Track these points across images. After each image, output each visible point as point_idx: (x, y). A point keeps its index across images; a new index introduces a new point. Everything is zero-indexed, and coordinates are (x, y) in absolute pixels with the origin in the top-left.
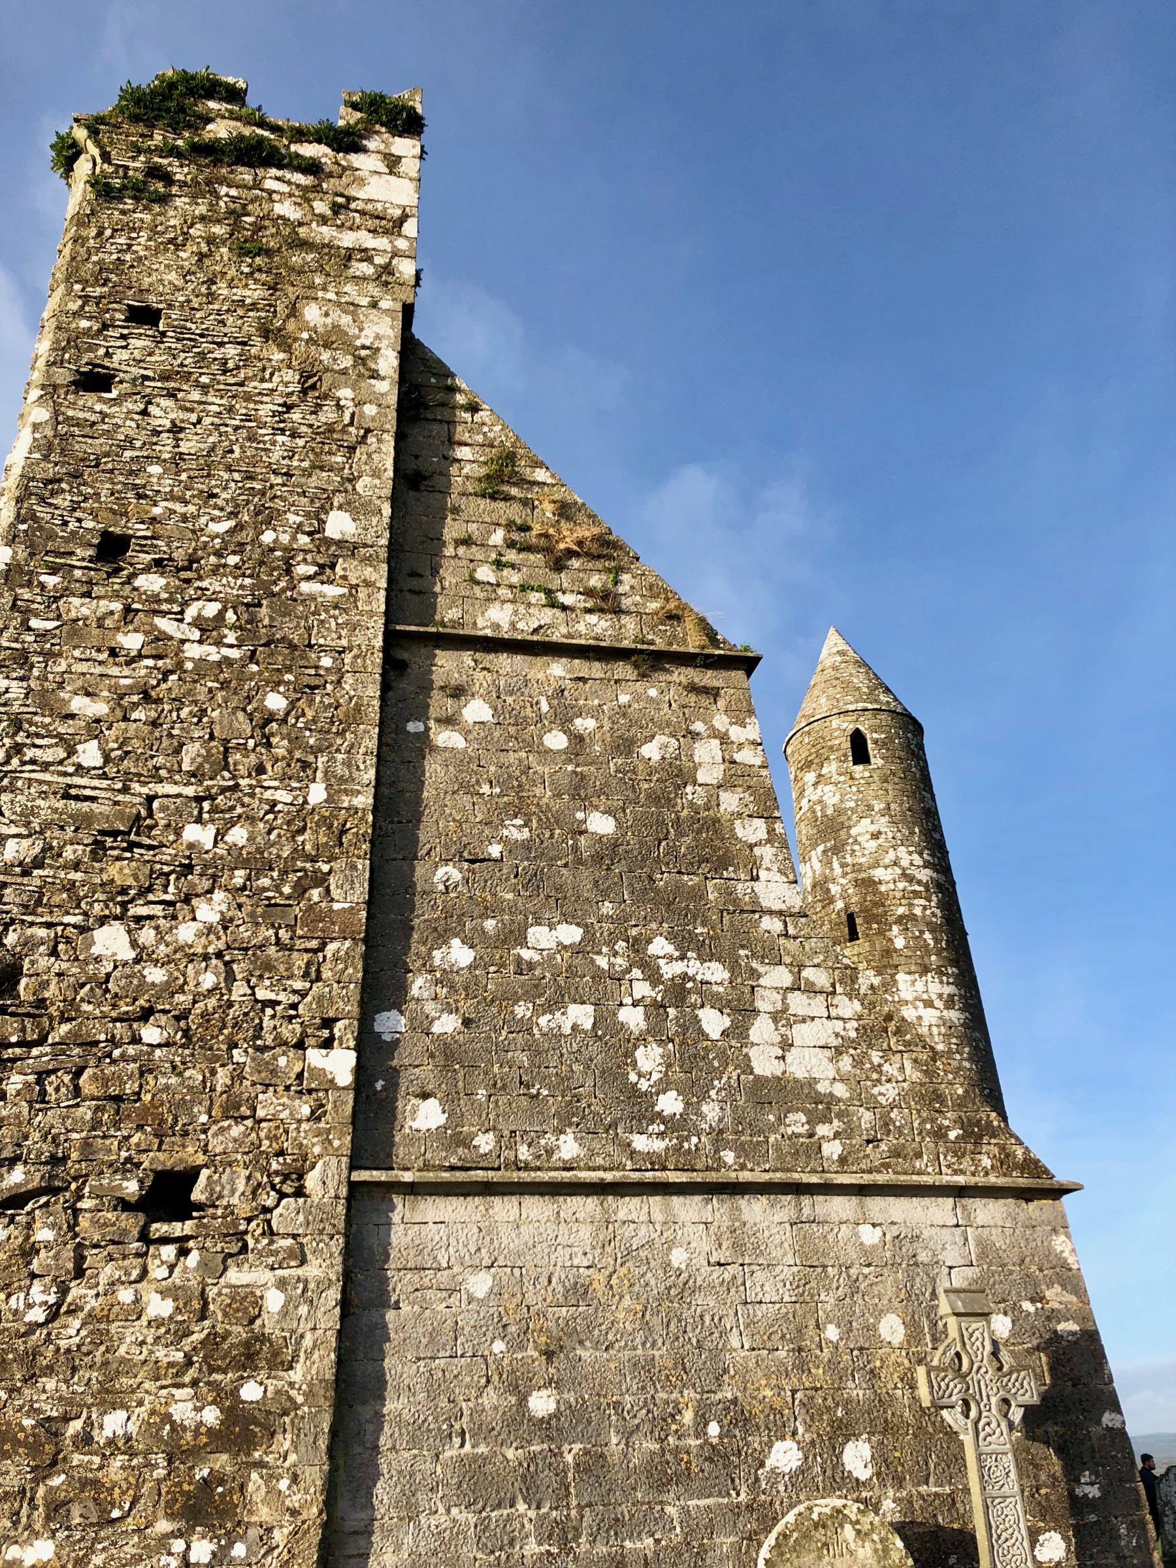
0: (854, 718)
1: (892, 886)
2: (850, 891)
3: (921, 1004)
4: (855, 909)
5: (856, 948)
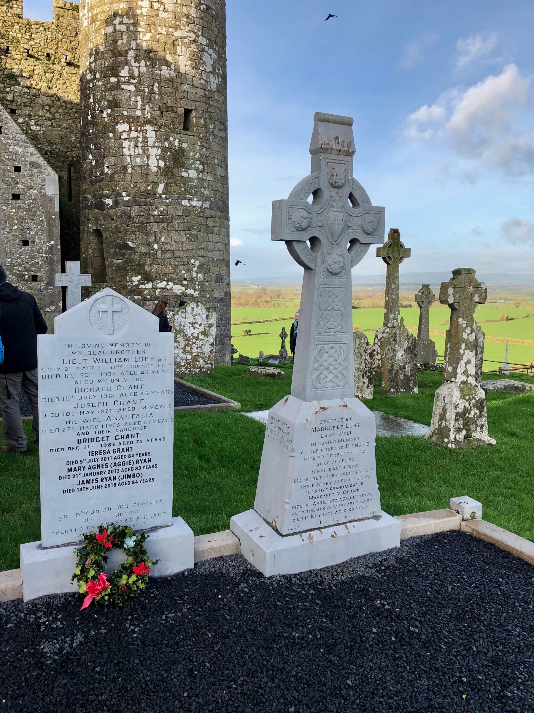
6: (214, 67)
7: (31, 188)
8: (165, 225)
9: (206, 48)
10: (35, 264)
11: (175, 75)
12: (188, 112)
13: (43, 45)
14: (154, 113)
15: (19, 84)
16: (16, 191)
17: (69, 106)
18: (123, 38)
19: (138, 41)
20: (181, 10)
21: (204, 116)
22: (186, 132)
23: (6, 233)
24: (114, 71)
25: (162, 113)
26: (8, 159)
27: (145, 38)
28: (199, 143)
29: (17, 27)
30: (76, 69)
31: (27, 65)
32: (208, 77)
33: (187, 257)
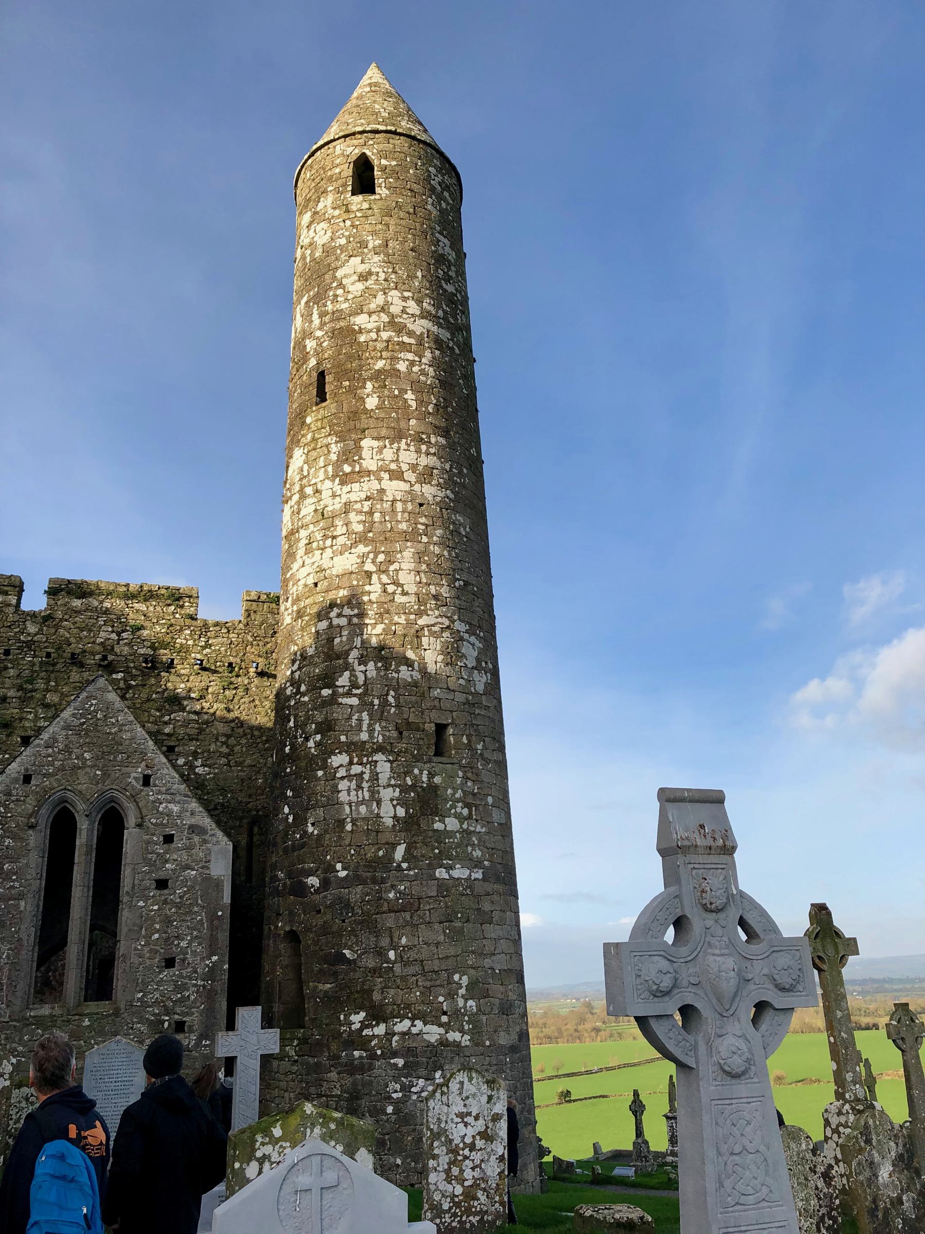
0: (362, 141)
1: (373, 335)
2: (325, 344)
3: (386, 476)
4: (327, 365)
5: (321, 411)
6: (478, 660)
7: (188, 867)
8: (407, 916)
9: (466, 636)
11: (419, 677)
12: (441, 729)
13: (223, 653)
14: (387, 734)
15: (183, 709)
16: (162, 875)
17: (256, 733)
18: (343, 634)
19: (365, 637)
20: (427, 590)
21: (467, 732)
22: (440, 759)
23: (139, 947)
24: (328, 680)
25: (401, 733)
26: (155, 825)
27: (374, 632)
28: (460, 774)
29: (188, 632)
30: (271, 679)
31: (197, 682)
32: (470, 674)
33: (446, 970)
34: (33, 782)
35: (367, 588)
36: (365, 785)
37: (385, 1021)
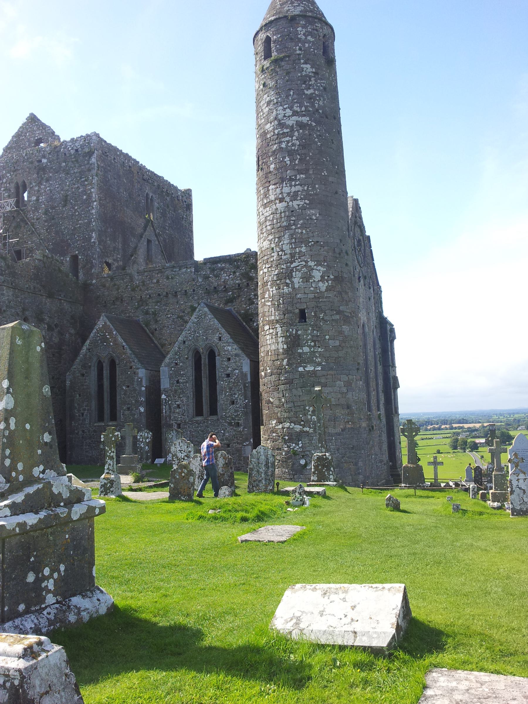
3: (278, 201)
6: (322, 277)
10: (237, 415)
16: (228, 372)
20: (294, 251)
21: (315, 310)
28: (310, 328)
34: (186, 343)
35: (273, 254)
36: (274, 337)
37: (282, 423)
